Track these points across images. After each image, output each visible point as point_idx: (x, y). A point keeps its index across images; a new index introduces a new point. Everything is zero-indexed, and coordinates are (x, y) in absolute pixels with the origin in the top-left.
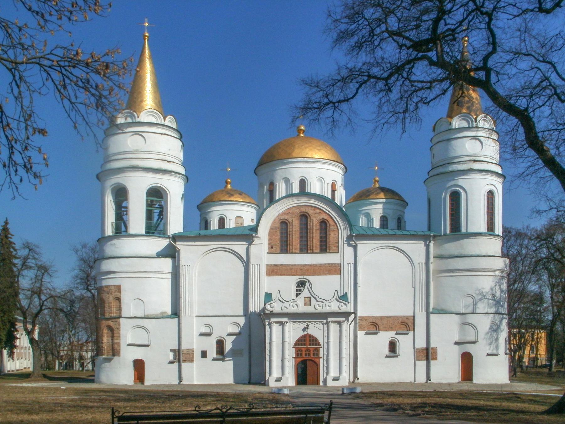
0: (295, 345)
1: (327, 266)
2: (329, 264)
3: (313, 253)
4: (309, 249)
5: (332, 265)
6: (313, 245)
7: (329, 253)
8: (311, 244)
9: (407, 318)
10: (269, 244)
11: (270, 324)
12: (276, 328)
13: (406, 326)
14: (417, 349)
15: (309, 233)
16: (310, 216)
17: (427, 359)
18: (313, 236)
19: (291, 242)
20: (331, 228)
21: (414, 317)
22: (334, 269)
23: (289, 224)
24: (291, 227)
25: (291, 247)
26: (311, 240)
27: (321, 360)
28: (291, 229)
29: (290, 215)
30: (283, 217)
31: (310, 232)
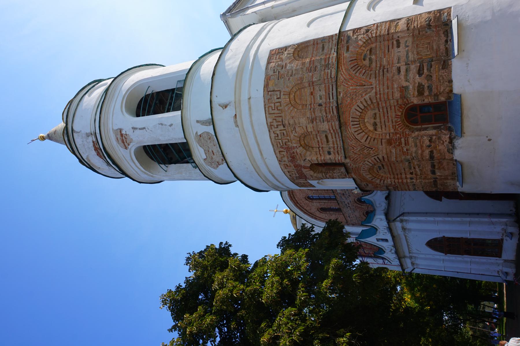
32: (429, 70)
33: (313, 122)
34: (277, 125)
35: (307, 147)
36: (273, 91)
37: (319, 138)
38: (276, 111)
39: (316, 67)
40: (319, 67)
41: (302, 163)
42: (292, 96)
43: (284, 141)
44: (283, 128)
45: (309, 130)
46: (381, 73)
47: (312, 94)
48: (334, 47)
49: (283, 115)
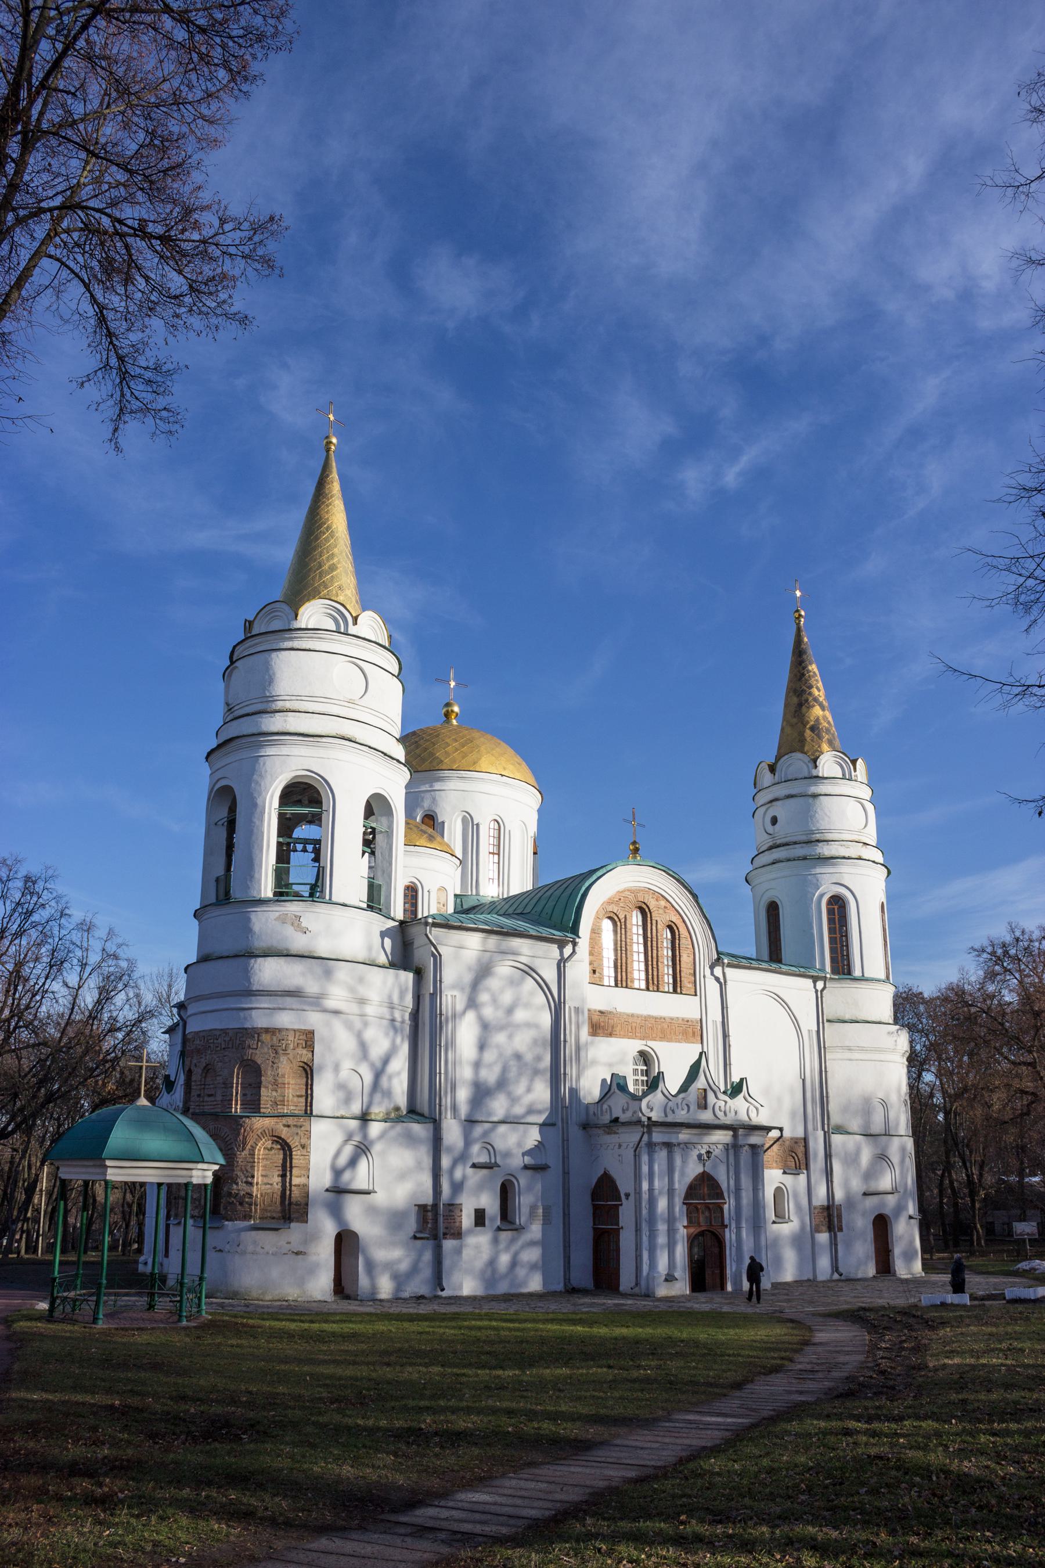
0: (686, 1198)
1: (680, 1021)
2: (683, 1020)
3: (658, 991)
4: (651, 982)
5: (688, 1021)
6: (658, 975)
7: (681, 993)
8: (655, 973)
9: (795, 1141)
10: (590, 964)
11: (651, 1146)
12: (662, 1155)
13: (794, 1158)
14: (815, 1208)
15: (650, 949)
16: (651, 913)
17: (830, 1228)
18: (657, 956)
19: (624, 964)
20: (683, 941)
21: (805, 1140)
22: (690, 1030)
23: (619, 923)
24: (623, 930)
25: (624, 974)
26: (655, 963)
27: (727, 1230)
28: (623, 936)
29: (622, 905)
30: (610, 908)
31: (652, 946)
32: (247, 1203)
33: (224, 1084)
34: (225, 1041)
35: (207, 1069)
36: (258, 1040)
37: (212, 1086)
38: (238, 1042)
39: (276, 1091)
40: (274, 1094)
41: (194, 1061)
42: (250, 1062)
43: (212, 1045)
44: (223, 1046)
45: (218, 1078)
46: (251, 1160)
47: (250, 1085)
48: (299, 1108)
49: (234, 1050)
